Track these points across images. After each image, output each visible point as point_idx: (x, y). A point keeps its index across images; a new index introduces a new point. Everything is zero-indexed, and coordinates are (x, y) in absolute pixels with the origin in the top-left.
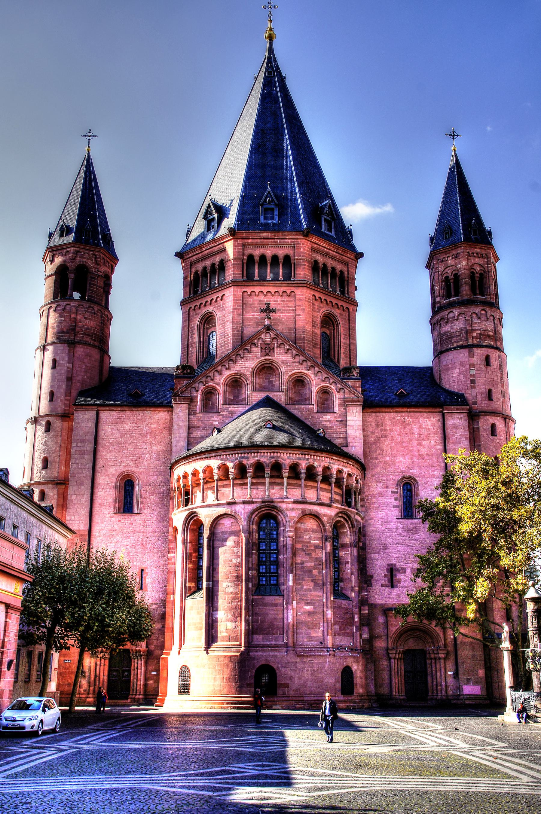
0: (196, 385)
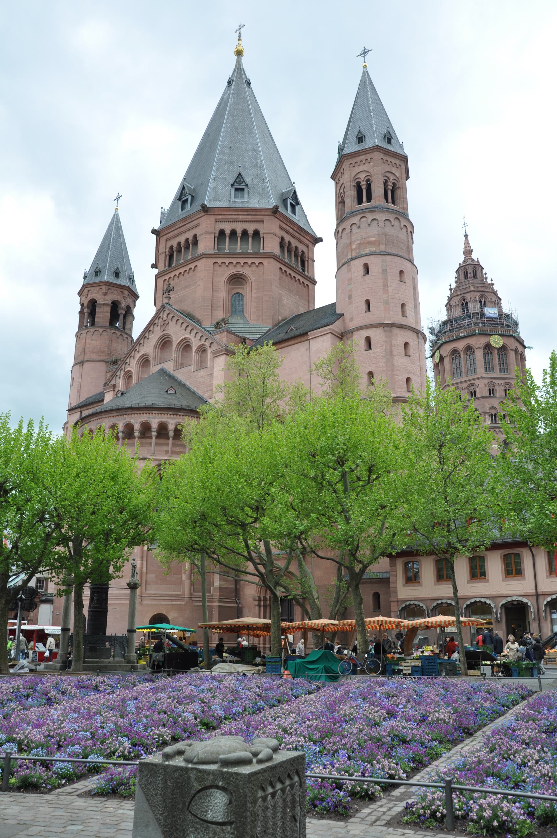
0: (118, 374)
